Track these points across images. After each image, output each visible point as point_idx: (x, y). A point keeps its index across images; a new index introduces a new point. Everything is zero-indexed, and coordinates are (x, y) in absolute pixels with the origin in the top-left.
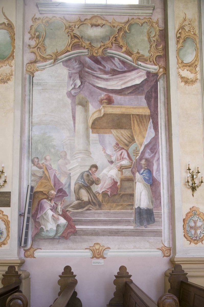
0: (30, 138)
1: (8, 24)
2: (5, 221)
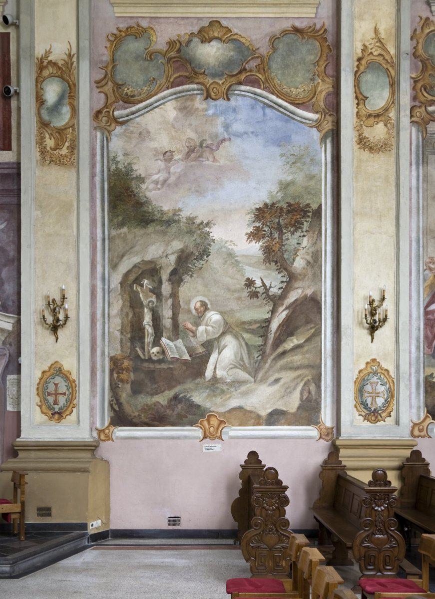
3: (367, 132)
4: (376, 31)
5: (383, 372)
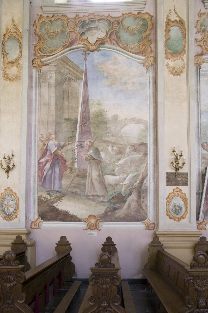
0: (200, 125)
1: (179, 21)
2: (183, 198)
3: (8, 71)
4: (13, 20)
5: (13, 194)
